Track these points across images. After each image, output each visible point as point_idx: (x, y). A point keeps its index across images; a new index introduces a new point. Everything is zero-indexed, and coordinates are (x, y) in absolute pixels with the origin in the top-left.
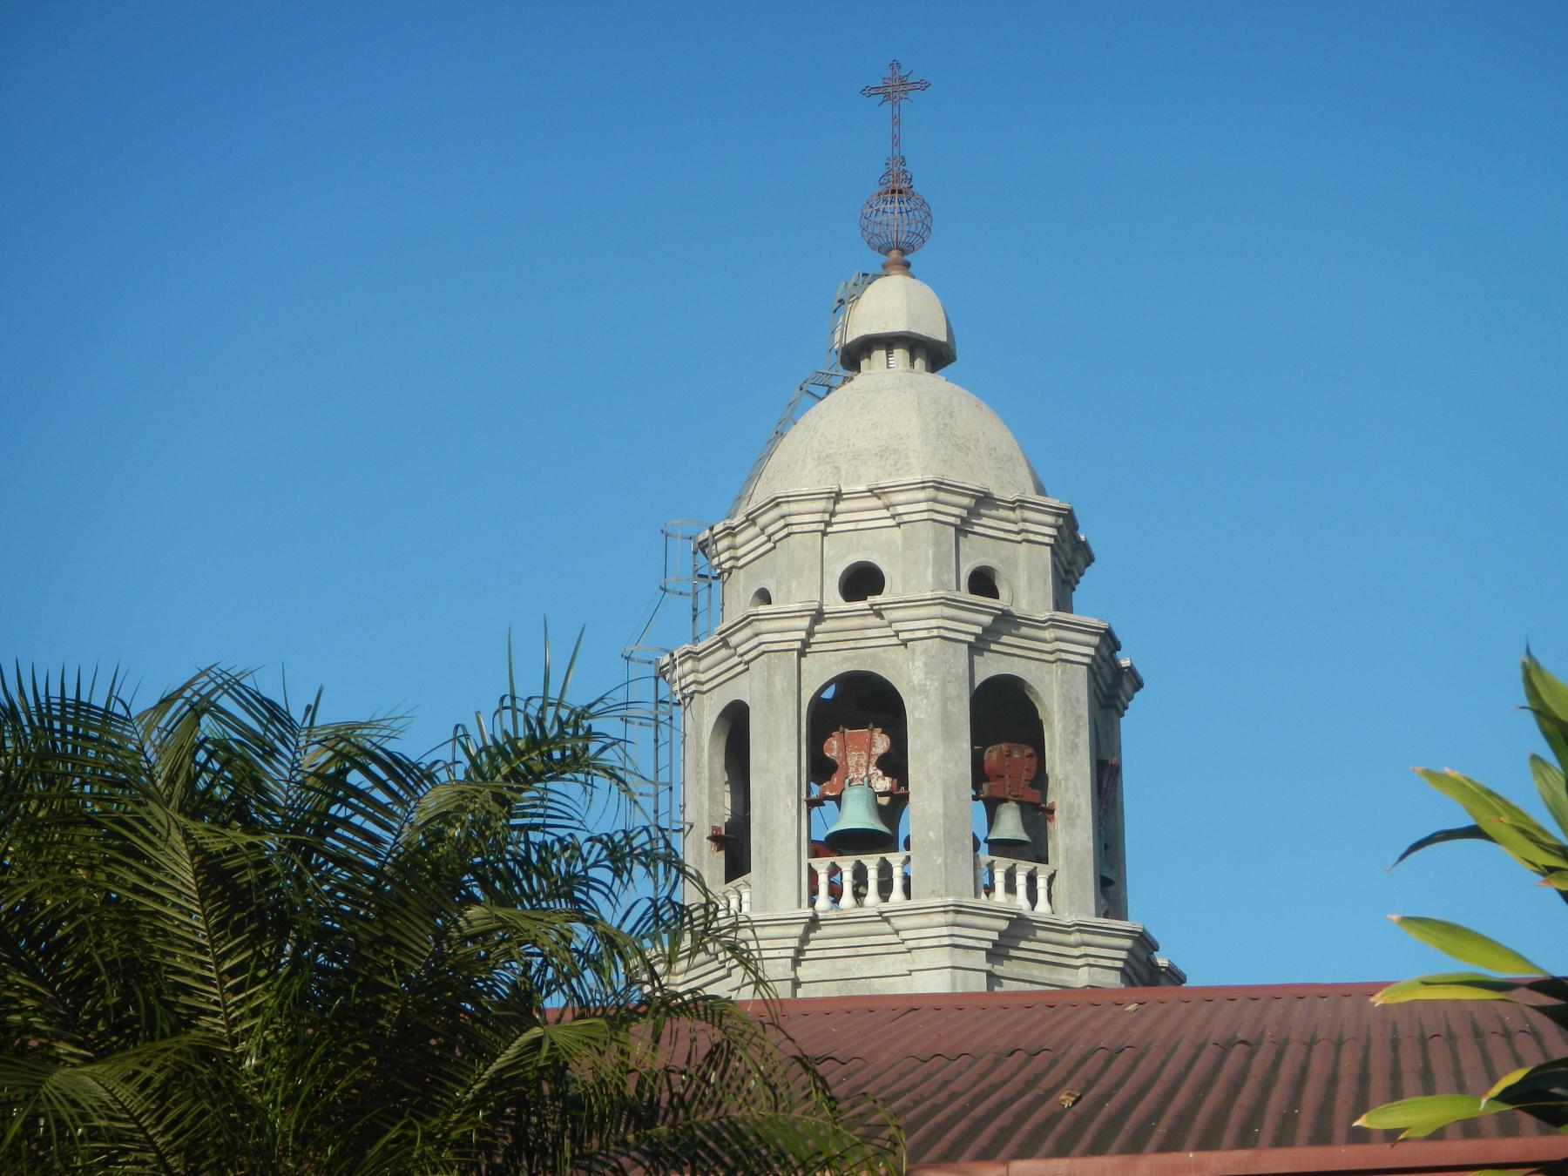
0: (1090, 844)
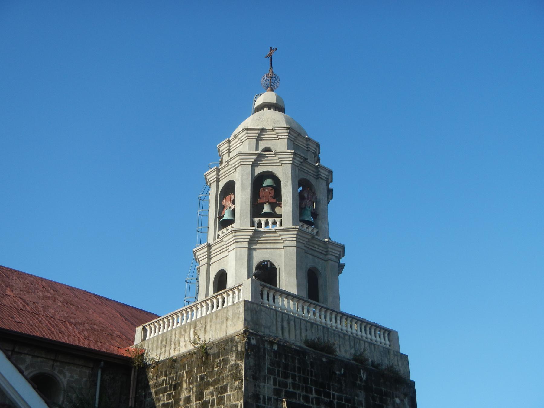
0: (291, 210)
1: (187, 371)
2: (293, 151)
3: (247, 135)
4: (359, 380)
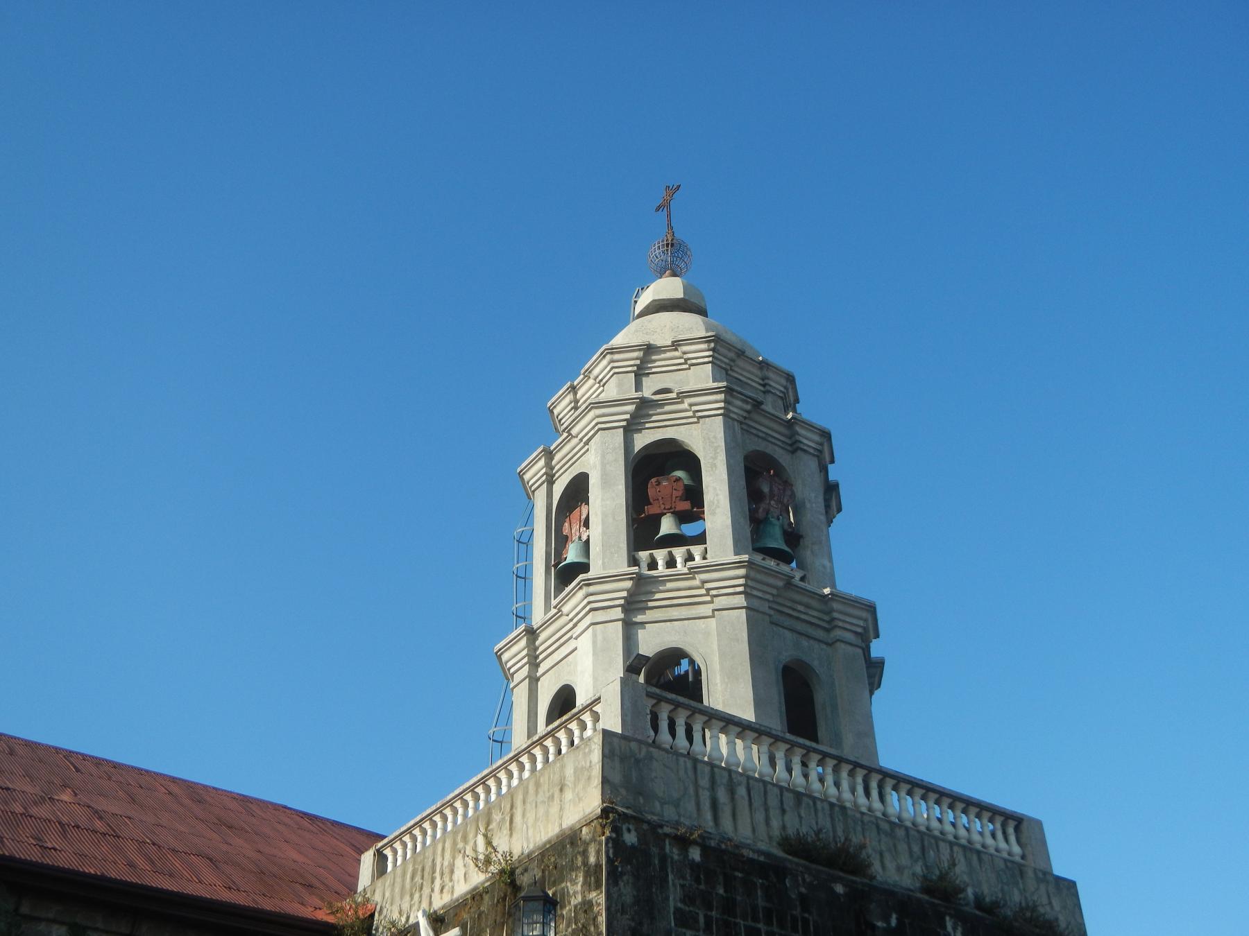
2: (725, 384)
3: (612, 365)
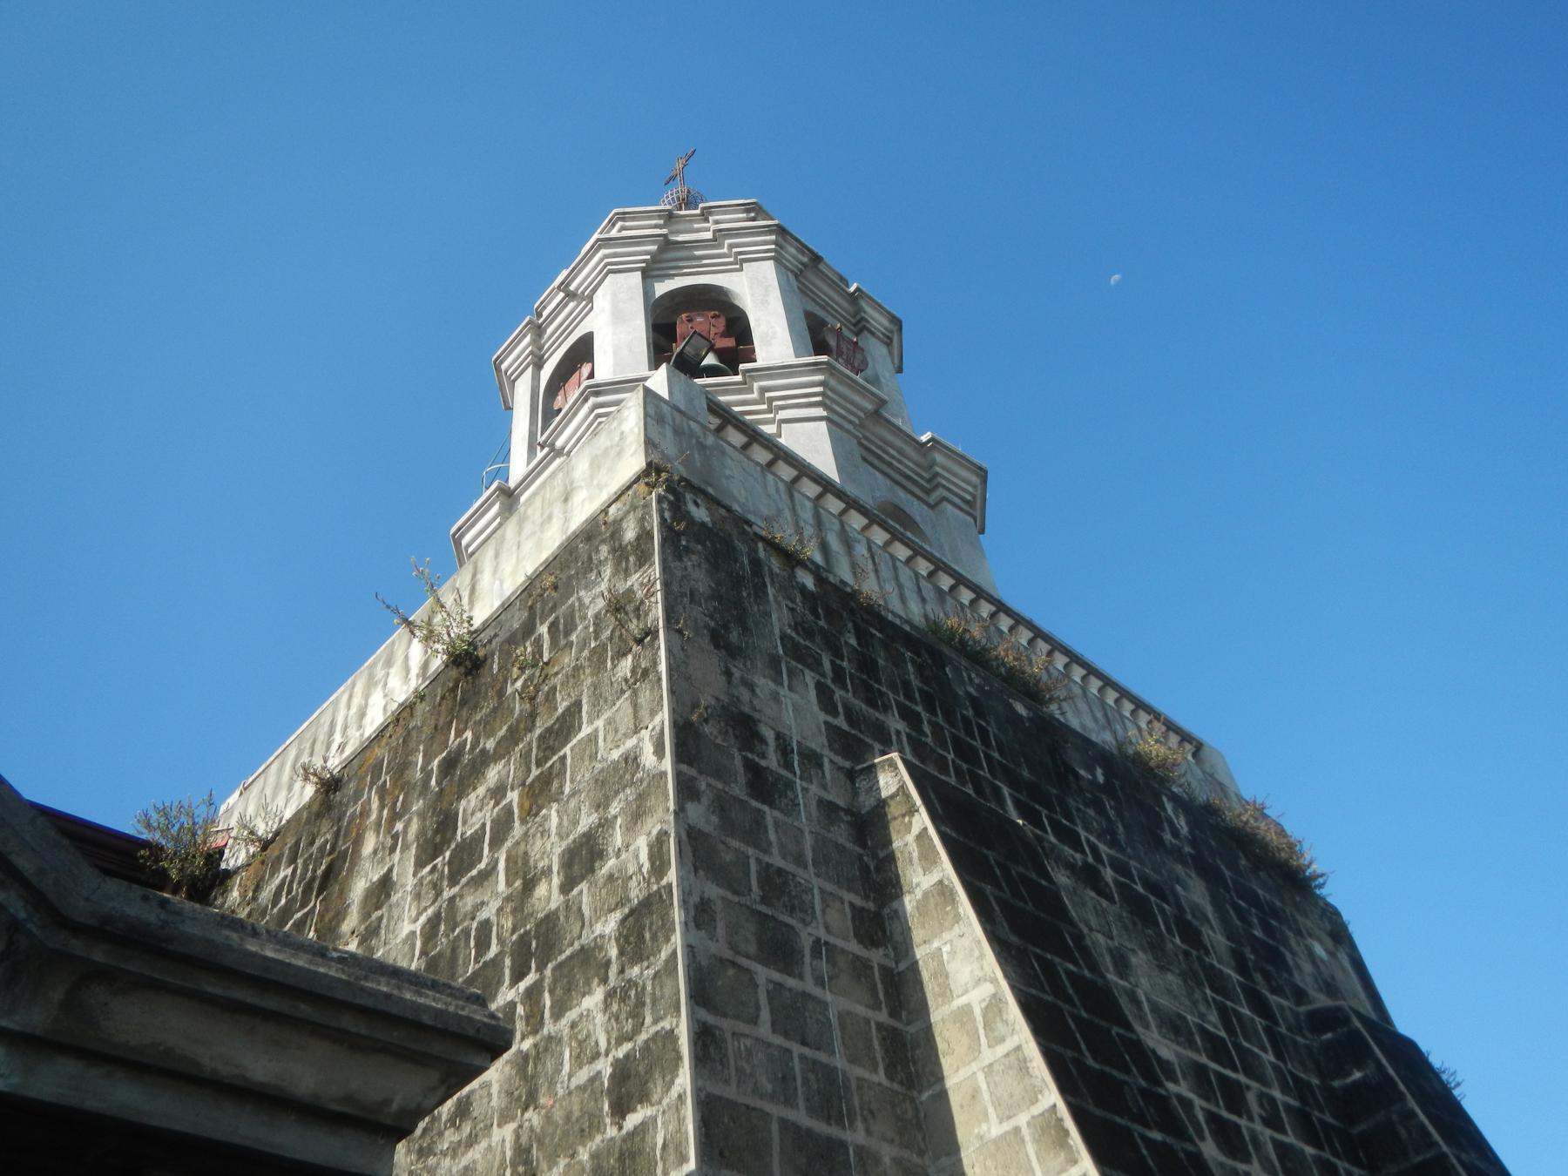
1: (385, 782)
4: (1167, 828)
